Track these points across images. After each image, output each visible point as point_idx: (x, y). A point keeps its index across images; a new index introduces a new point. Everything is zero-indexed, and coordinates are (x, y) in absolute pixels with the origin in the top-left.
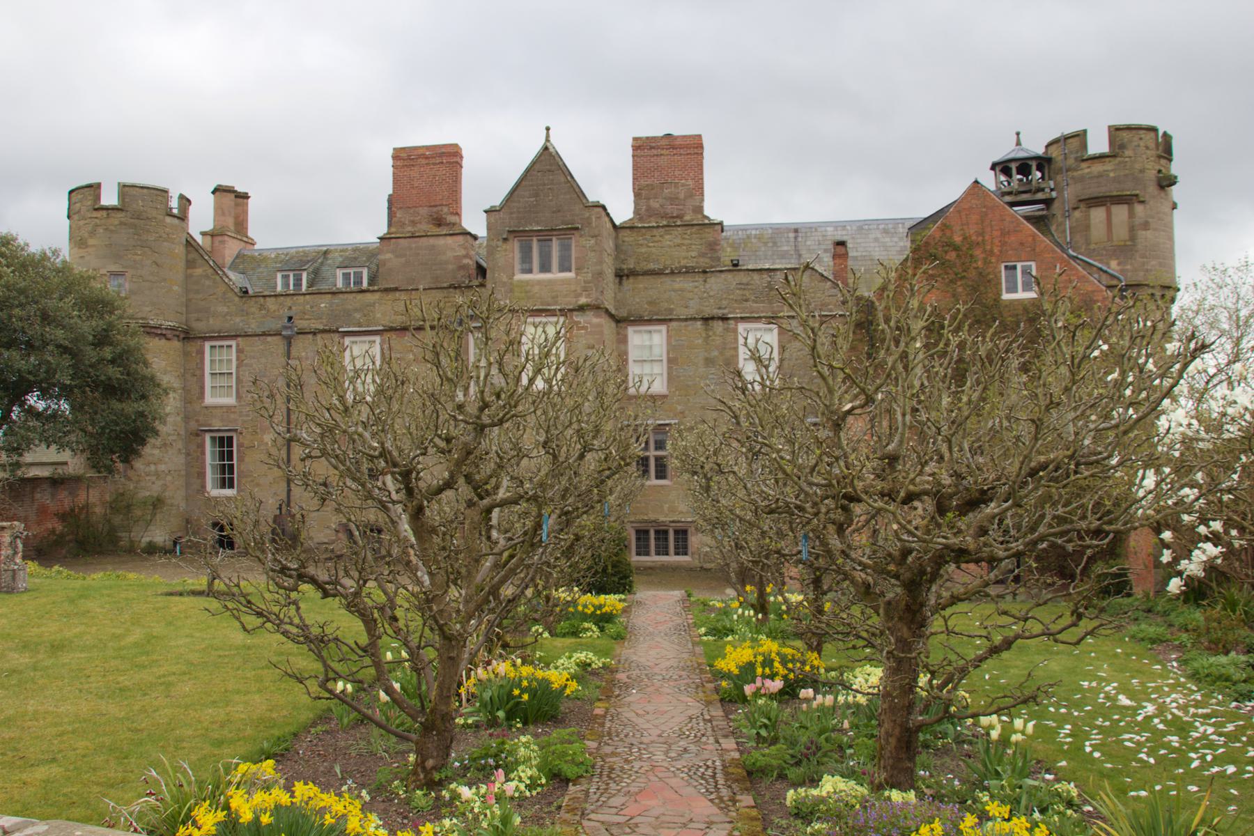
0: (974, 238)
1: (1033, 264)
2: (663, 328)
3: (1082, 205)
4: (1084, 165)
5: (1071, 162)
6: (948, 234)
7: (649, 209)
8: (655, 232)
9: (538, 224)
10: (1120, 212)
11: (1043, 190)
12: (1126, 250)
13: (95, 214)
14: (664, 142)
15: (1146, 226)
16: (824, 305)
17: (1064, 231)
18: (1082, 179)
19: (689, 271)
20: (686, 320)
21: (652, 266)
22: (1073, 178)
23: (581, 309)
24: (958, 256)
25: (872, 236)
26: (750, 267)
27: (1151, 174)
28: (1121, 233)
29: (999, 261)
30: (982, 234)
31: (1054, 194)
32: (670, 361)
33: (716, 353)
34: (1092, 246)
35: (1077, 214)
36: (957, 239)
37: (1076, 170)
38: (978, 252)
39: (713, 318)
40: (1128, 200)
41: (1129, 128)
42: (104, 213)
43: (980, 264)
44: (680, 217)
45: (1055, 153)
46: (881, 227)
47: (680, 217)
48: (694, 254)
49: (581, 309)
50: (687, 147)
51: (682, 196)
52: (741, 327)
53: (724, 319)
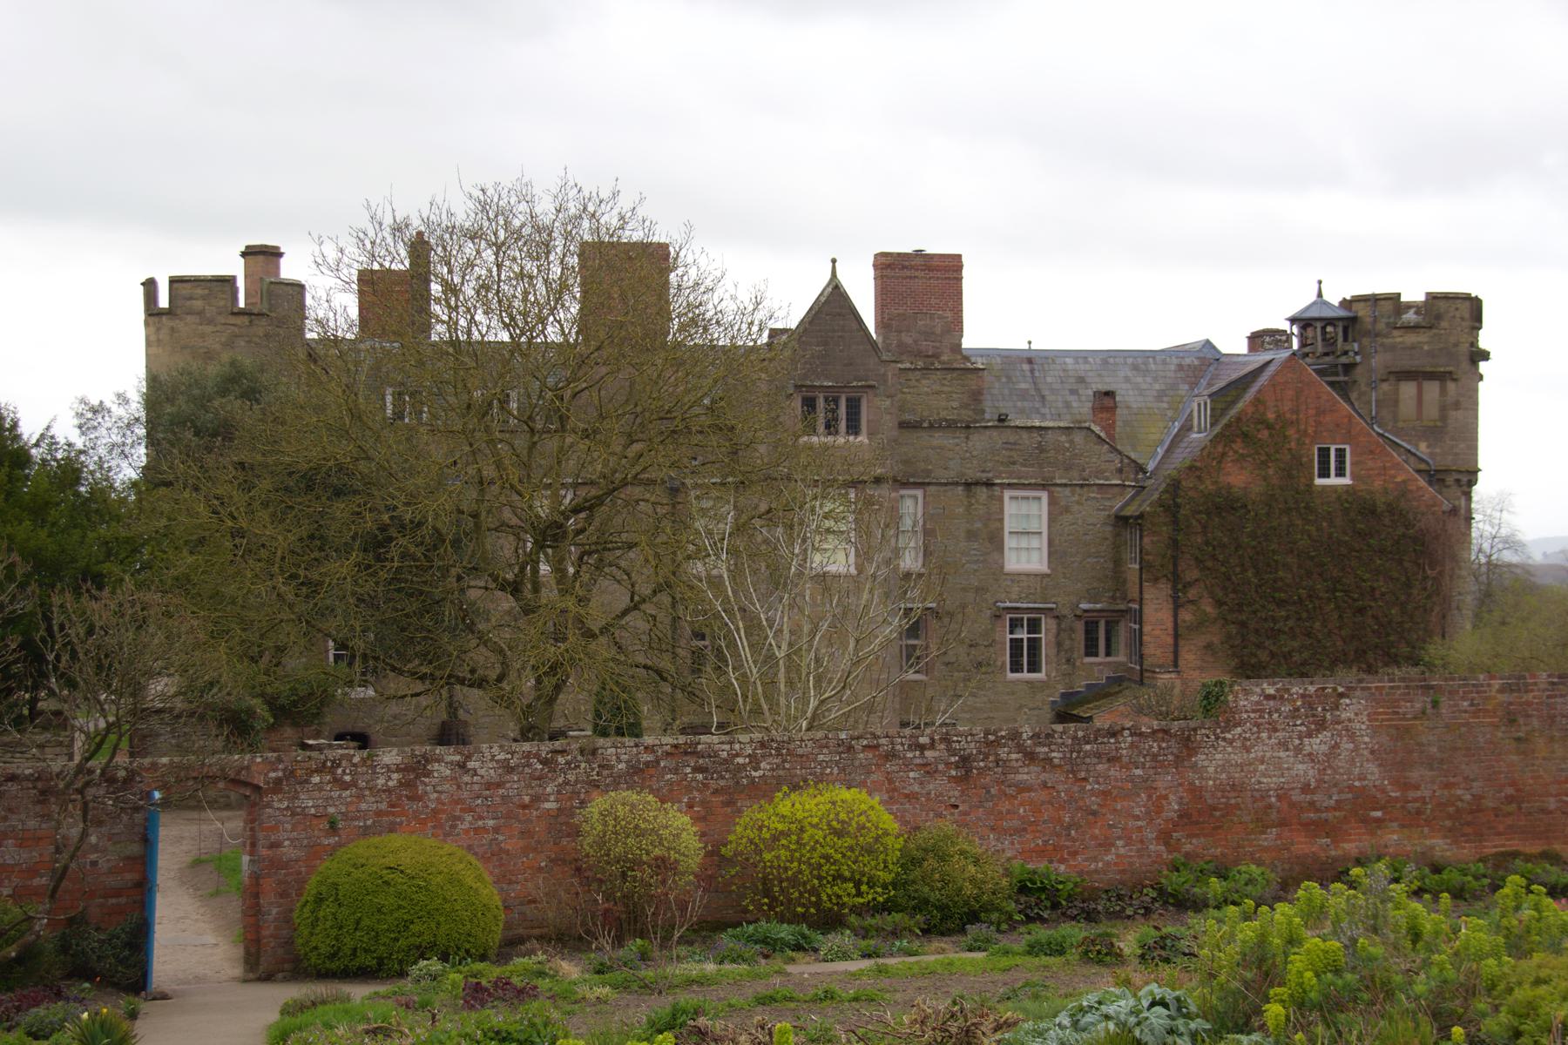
0: (1288, 416)
1: (1347, 447)
2: (919, 493)
3: (1392, 378)
4: (1396, 333)
5: (1381, 326)
6: (1261, 409)
7: (900, 344)
8: (910, 375)
9: (827, 378)
10: (1432, 389)
11: (1346, 353)
12: (1435, 432)
13: (233, 320)
14: (918, 261)
15: (1457, 405)
16: (1099, 473)
17: (1369, 402)
18: (1393, 348)
19: (950, 425)
20: (946, 484)
21: (907, 417)
22: (1382, 345)
23: (878, 480)
24: (1271, 436)
25: (1122, 374)
26: (1018, 423)
27: (1464, 348)
28: (1431, 411)
29: (1313, 443)
30: (1297, 412)
31: (1358, 359)
32: (927, 533)
33: (978, 525)
34: (1400, 424)
35: (1385, 386)
36: (1271, 416)
37: (1386, 336)
38: (1291, 432)
39: (977, 484)
40: (1442, 377)
41: (1447, 297)
42: (246, 319)
43: (1293, 444)
44: (936, 356)
45: (1361, 311)
46: (1130, 361)
47: (936, 356)
48: (955, 404)
49: (878, 480)
50: (946, 269)
51: (938, 330)
52: (1007, 494)
53: (989, 484)
